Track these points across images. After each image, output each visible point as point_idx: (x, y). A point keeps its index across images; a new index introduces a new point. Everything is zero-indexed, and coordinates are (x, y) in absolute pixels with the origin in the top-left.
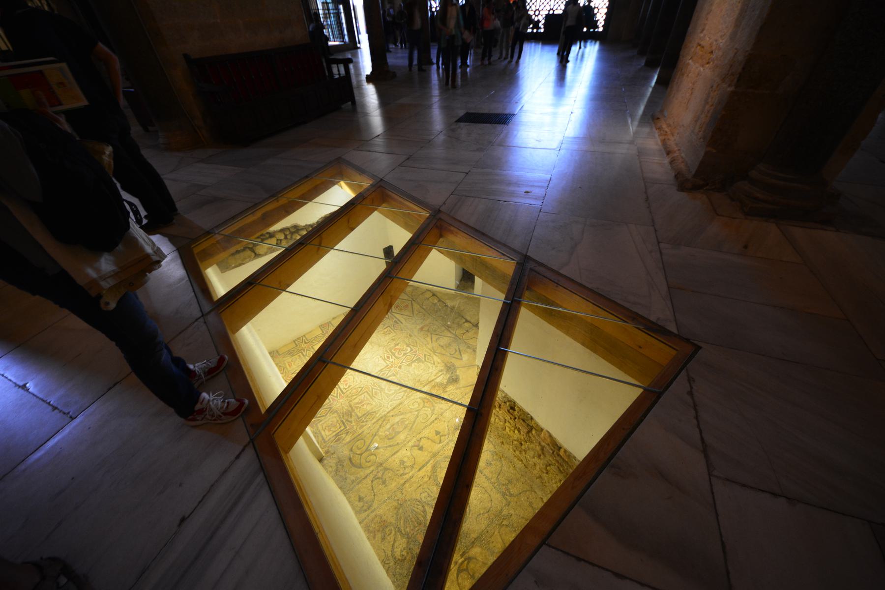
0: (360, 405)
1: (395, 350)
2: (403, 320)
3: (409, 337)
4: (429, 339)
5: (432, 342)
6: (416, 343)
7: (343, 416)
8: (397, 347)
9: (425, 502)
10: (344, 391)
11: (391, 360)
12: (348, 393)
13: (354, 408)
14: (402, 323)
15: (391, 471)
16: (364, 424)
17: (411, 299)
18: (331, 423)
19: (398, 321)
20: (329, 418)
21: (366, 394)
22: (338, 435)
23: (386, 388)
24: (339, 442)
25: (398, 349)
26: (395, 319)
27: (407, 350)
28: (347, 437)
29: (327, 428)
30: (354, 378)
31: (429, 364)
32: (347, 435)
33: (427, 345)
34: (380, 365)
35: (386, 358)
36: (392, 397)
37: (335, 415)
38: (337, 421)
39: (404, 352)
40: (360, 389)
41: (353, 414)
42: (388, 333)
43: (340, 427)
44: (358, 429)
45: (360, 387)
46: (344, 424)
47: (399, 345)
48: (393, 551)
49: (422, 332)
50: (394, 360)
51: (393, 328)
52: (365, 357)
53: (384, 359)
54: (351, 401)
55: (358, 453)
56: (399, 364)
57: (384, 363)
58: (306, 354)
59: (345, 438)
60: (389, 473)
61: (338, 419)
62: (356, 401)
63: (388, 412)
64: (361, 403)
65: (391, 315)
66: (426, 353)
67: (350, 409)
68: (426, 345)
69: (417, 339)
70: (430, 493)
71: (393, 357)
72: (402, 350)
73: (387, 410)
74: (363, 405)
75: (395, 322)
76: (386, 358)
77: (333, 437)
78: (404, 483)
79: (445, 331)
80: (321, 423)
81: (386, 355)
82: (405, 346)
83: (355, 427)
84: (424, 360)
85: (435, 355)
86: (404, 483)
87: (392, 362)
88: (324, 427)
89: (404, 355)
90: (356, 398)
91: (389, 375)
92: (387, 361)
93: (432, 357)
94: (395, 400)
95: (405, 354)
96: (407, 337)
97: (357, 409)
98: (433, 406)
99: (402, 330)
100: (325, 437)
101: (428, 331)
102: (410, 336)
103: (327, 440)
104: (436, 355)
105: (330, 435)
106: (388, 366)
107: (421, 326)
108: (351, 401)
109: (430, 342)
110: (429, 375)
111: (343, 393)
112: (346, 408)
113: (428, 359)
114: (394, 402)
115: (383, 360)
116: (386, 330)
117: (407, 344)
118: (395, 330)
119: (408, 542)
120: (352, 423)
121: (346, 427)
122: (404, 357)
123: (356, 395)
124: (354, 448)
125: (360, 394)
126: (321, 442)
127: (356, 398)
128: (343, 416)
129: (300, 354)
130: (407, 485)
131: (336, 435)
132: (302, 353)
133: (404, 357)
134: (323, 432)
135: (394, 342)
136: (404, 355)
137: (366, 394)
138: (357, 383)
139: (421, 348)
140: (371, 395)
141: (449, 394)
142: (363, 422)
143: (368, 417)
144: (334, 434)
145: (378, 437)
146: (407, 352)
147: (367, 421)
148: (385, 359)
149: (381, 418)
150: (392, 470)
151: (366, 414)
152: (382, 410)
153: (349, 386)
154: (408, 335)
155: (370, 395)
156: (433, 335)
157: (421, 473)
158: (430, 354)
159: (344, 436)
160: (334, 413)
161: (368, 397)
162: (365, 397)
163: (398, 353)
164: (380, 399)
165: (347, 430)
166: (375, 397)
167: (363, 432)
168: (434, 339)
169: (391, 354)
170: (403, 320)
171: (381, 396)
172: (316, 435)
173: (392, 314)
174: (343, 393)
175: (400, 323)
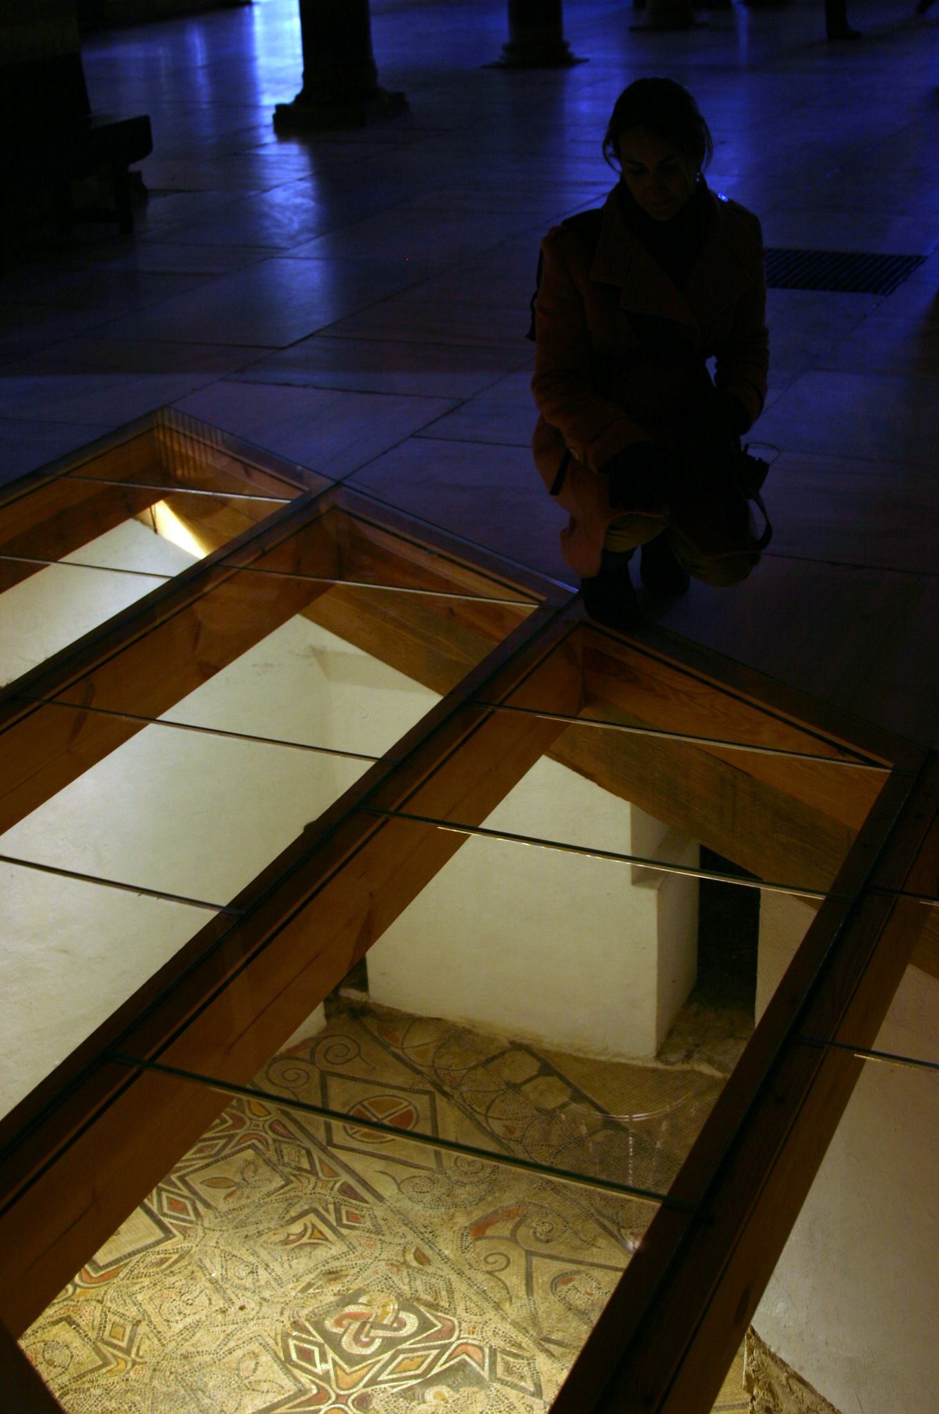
1: (338, 1323)
2: (388, 1189)
3: (414, 1264)
4: (514, 1279)
5: (530, 1289)
6: (450, 1291)
8: (351, 1309)
11: (320, 1368)
14: (380, 1198)
17: (429, 1087)
19: (359, 1189)
25: (355, 1317)
26: (345, 1178)
27: (403, 1324)
31: (513, 1394)
33: (507, 1306)
34: (265, 1386)
35: (294, 1356)
39: (389, 1334)
42: (305, 1240)
47: (363, 1299)
49: (479, 1243)
50: (335, 1364)
51: (332, 1218)
52: (187, 1347)
53: (286, 1363)
56: (358, 1391)
65: (324, 1157)
66: (498, 1343)
68: (497, 1306)
69: (454, 1277)
71: (331, 1354)
72: (377, 1325)
75: (347, 1191)
76: (294, 1356)
79: (602, 1242)
82: (393, 1306)
84: (485, 1374)
85: (547, 1351)
87: (325, 1377)
89: (381, 1350)
92: (296, 1372)
93: (530, 1360)
95: (389, 1344)
96: (405, 1263)
99: (378, 1232)
101: (513, 1238)
102: (422, 1258)
104: (551, 1354)
106: (302, 1392)
107: (477, 1214)
109: (522, 1292)
113: (509, 1369)
116: (296, 1228)
117: (399, 1296)
118: (344, 1231)
122: (387, 1356)
133: (387, 1356)
135: (337, 1287)
136: (381, 1350)
139: (475, 1318)
146: (404, 1332)
154: (410, 1257)
156: (536, 1261)
158: (520, 1346)
163: (356, 1339)
168: (542, 1279)
169: (319, 1339)
170: (388, 1189)
173: (333, 1157)
175: (368, 1196)
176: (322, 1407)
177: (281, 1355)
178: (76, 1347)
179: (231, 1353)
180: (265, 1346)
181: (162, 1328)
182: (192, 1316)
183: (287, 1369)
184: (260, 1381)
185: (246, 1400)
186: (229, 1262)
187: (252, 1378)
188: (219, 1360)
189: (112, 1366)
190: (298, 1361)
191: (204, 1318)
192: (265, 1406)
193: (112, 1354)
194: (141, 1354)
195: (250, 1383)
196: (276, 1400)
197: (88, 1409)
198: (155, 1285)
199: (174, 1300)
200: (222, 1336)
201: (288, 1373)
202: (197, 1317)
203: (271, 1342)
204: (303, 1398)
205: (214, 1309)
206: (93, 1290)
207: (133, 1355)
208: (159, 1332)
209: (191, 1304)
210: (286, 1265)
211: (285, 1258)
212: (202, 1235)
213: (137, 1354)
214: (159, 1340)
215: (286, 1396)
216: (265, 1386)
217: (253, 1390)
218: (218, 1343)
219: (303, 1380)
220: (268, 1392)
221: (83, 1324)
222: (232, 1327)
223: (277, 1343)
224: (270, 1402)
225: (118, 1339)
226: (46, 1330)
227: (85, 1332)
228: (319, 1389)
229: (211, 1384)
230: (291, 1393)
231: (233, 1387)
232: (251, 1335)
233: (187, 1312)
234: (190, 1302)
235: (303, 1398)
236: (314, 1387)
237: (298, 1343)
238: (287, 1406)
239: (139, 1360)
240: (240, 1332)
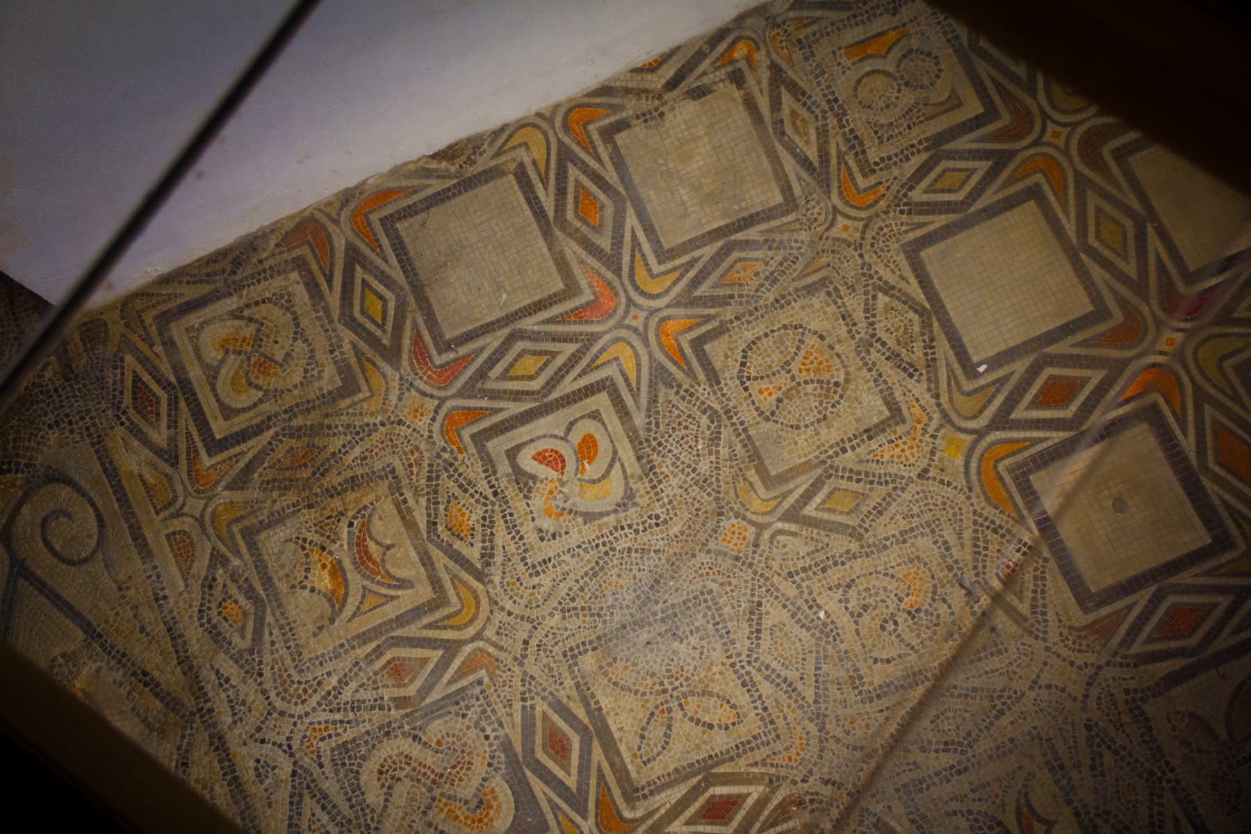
0: (342, 551)
7: (296, 433)
10: (497, 446)
12: (473, 469)
13: (336, 503)
16: (200, 566)
18: (279, 357)
20: (320, 343)
21: (425, 592)
22: (173, 405)
23: (416, 751)
24: (127, 400)
28: (146, 454)
29: (249, 330)
30: (589, 517)
32: (159, 452)
34: (655, 732)
36: (330, 786)
37: (329, 378)
38: (278, 394)
40: (473, 553)
41: (291, 497)
43: (228, 412)
44: (176, 525)
45: (487, 555)
46: (241, 437)
53: (707, 772)
54: (396, 488)
55: (26, 510)
57: (657, 770)
58: (951, 155)
59: (146, 442)
61: (289, 401)
62: (386, 526)
63: (219, 744)
64: (363, 558)
67: (332, 479)
73: (234, 738)
74: (337, 570)
77: (178, 368)
80: (301, 295)
81: (755, 792)
83: (195, 505)
88: (260, 312)
90: (410, 525)
91: (538, 786)
94: (295, 801)
97: (320, 527)
100: (194, 319)
103: (176, 331)
105: (197, 349)
108: (396, 488)
111: (481, 439)
112: (357, 451)
114: (283, 794)
115: (695, 757)
120: (229, 487)
121: (215, 446)
123: (432, 525)
124: (64, 492)
125: (436, 553)
126: (170, 297)
127: (410, 525)
128: (296, 433)
129: (974, 108)
131: (186, 386)
132: (975, 123)
134: (233, 303)
137: (425, 592)
138: (531, 538)
140: (398, 633)
142: (218, 559)
143: (233, 590)
144: (195, 373)
145: (70, 647)
147: (209, 583)
148: (711, 780)
149: (198, 690)
151: (267, 581)
152: (253, 697)
153: (524, 481)
155: (401, 621)
159: (160, 436)
160: (344, 370)
161: (390, 612)
162: (403, 584)
164: (347, 695)
165: (193, 453)
166: (370, 659)
167: (146, 552)
171: (355, 706)
172: (226, 264)
174: (481, 439)
176: (591, 820)
177: (721, 769)
178: (817, 433)
179: (744, 684)
180: (742, 748)
181: (835, 575)
182: (854, 626)
183: (688, 777)
184: (669, 727)
185: (629, 701)
186: (986, 703)
187: (678, 714)
188: (732, 665)
189: (761, 490)
190: (707, 795)
191: (842, 647)
192: (613, 728)
193: (791, 492)
194: (780, 538)
195: (670, 710)
196: (622, 748)
197: (670, 451)
198: (950, 569)
199: (901, 600)
200: (792, 675)
201: (678, 776)
202: (849, 635)
203: (758, 755)
204: (617, 793)
205: (861, 665)
206: (959, 461)
207: (780, 525)
208: (824, 570)
209: (883, 628)
210: (954, 806)
211: (975, 807)
212: (1079, 662)
213: (781, 532)
214: (804, 569)
215: (629, 767)
216: (655, 732)
217: (652, 714)
218: (774, 665)
219: (659, 798)
220: (642, 737)
221: (874, 445)
222: (809, 693)
223: (756, 764)
224: (621, 740)
225: (824, 502)
226: (872, 384)
227: (853, 448)
228: (633, 821)
229: (682, 648)
230: (634, 775)
231: (666, 682)
232: (780, 723)
233: (866, 619)
234: (890, 627)
235: (617, 793)
236: (639, 814)
237: (750, 802)
238: (605, 765)
239: (766, 535)
240: (794, 705)
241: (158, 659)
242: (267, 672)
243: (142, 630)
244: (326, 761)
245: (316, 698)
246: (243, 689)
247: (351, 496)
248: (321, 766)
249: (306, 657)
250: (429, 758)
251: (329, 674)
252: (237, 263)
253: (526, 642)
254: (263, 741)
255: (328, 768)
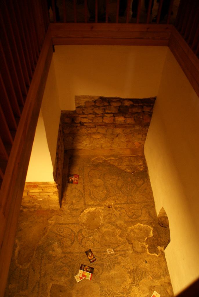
9: (119, 189)
15: (128, 214)
48: (143, 183)
60: (129, 214)
67: (135, 275)
70: (114, 191)
78: (124, 204)
86: (124, 204)
98: (78, 232)
110: (61, 260)
119: (136, 182)
130: (123, 202)
141: (62, 232)
150: (127, 215)
157: (112, 203)
241: (121, 248)
242: (115, 259)
243: (125, 247)
244: (103, 263)
245: (110, 263)
246: (114, 256)
247: (133, 277)
248: (102, 262)
249: (115, 264)
250: (98, 275)
251: (112, 266)
252: (166, 273)
253: (107, 292)
254: (107, 256)
255: (102, 262)
